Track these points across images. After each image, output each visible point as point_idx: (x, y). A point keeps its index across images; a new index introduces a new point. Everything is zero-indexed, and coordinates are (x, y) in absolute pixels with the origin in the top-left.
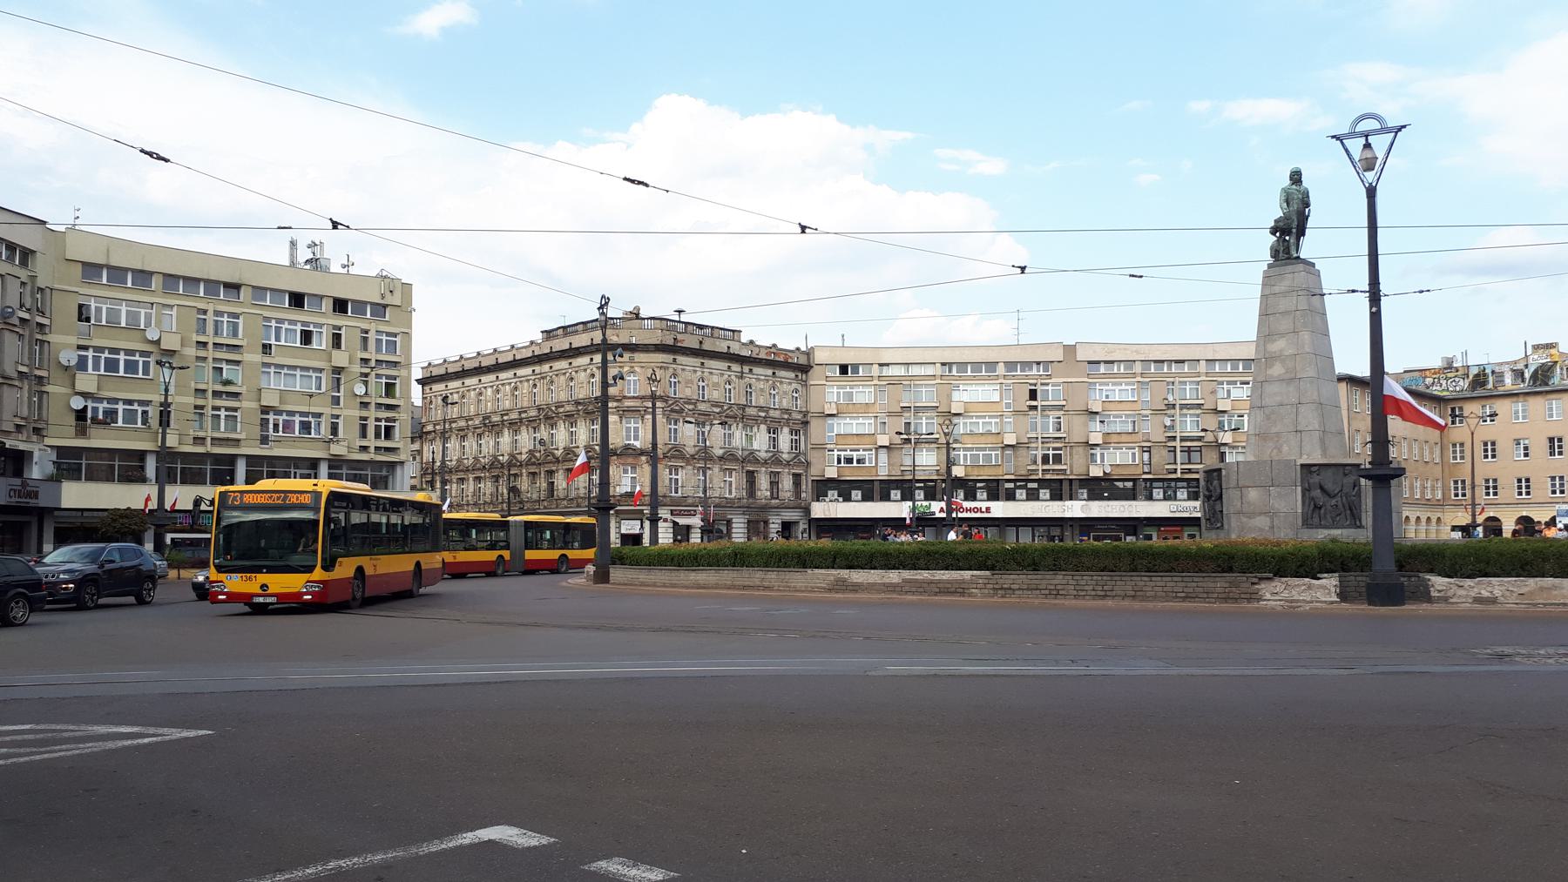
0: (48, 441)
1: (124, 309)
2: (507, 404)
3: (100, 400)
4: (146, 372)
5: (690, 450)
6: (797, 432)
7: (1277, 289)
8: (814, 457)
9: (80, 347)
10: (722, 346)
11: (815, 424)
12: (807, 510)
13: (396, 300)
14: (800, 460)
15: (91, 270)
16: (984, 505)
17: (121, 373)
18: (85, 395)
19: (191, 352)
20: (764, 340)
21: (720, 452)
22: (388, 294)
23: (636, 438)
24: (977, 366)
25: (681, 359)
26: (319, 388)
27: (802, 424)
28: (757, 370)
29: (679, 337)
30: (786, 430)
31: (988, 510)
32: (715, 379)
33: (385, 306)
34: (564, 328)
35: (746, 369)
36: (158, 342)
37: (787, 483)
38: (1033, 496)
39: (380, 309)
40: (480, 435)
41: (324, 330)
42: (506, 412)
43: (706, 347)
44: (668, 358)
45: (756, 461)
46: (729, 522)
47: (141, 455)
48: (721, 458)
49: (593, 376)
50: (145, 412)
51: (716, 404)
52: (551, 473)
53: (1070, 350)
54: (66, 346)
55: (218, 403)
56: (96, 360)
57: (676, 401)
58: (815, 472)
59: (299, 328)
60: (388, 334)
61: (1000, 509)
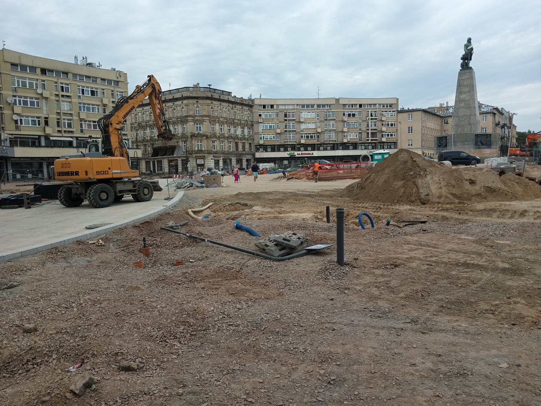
0: (6, 132)
1: (27, 81)
2: (148, 119)
3: (23, 116)
4: (38, 105)
5: (218, 135)
6: (250, 128)
7: (463, 78)
8: (256, 137)
9: (14, 96)
10: (226, 98)
11: (255, 125)
12: (254, 155)
13: (121, 79)
14: (251, 138)
15: (14, 65)
16: (311, 152)
17: (29, 106)
18: (17, 114)
19: (54, 98)
20: (238, 96)
21: (227, 135)
22: (119, 77)
23: (200, 130)
24: (308, 106)
25: (214, 102)
26: (98, 112)
27: (251, 126)
28: (237, 107)
29: (213, 94)
30: (246, 128)
31: (312, 154)
32: (224, 109)
33: (118, 82)
34: (170, 91)
35: (234, 106)
36: (42, 94)
37: (247, 146)
38: (325, 149)
39: (117, 83)
40: (137, 130)
41: (98, 90)
42: (148, 121)
43: (221, 98)
44: (209, 102)
45: (238, 138)
46: (231, 160)
47: (40, 136)
48: (228, 138)
49: (183, 108)
50: (39, 121)
51: (225, 118)
52: (145, 145)
53: (337, 100)
54: (9, 95)
55: (65, 117)
56: (20, 101)
57: (213, 117)
58: (256, 142)
59: (90, 89)
60: (120, 92)
61: (316, 153)
